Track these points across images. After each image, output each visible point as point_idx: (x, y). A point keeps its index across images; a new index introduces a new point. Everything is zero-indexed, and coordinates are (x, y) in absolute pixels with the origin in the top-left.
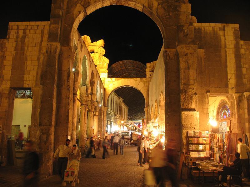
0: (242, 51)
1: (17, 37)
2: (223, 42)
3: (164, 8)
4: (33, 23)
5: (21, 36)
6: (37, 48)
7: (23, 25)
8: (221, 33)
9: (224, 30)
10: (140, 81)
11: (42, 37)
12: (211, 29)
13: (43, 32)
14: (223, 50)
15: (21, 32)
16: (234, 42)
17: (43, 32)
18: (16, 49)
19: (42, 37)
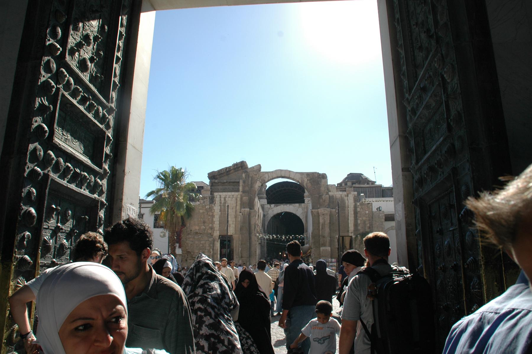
0: (358, 209)
1: (221, 203)
2: (347, 204)
3: (311, 183)
4: (229, 193)
5: (223, 202)
6: (234, 210)
7: (223, 194)
8: (346, 198)
9: (348, 196)
10: (299, 207)
11: (236, 203)
12: (340, 196)
13: (236, 199)
14: (346, 209)
15: (223, 199)
16: (354, 204)
17: (236, 199)
18: (220, 211)
19: (236, 203)
